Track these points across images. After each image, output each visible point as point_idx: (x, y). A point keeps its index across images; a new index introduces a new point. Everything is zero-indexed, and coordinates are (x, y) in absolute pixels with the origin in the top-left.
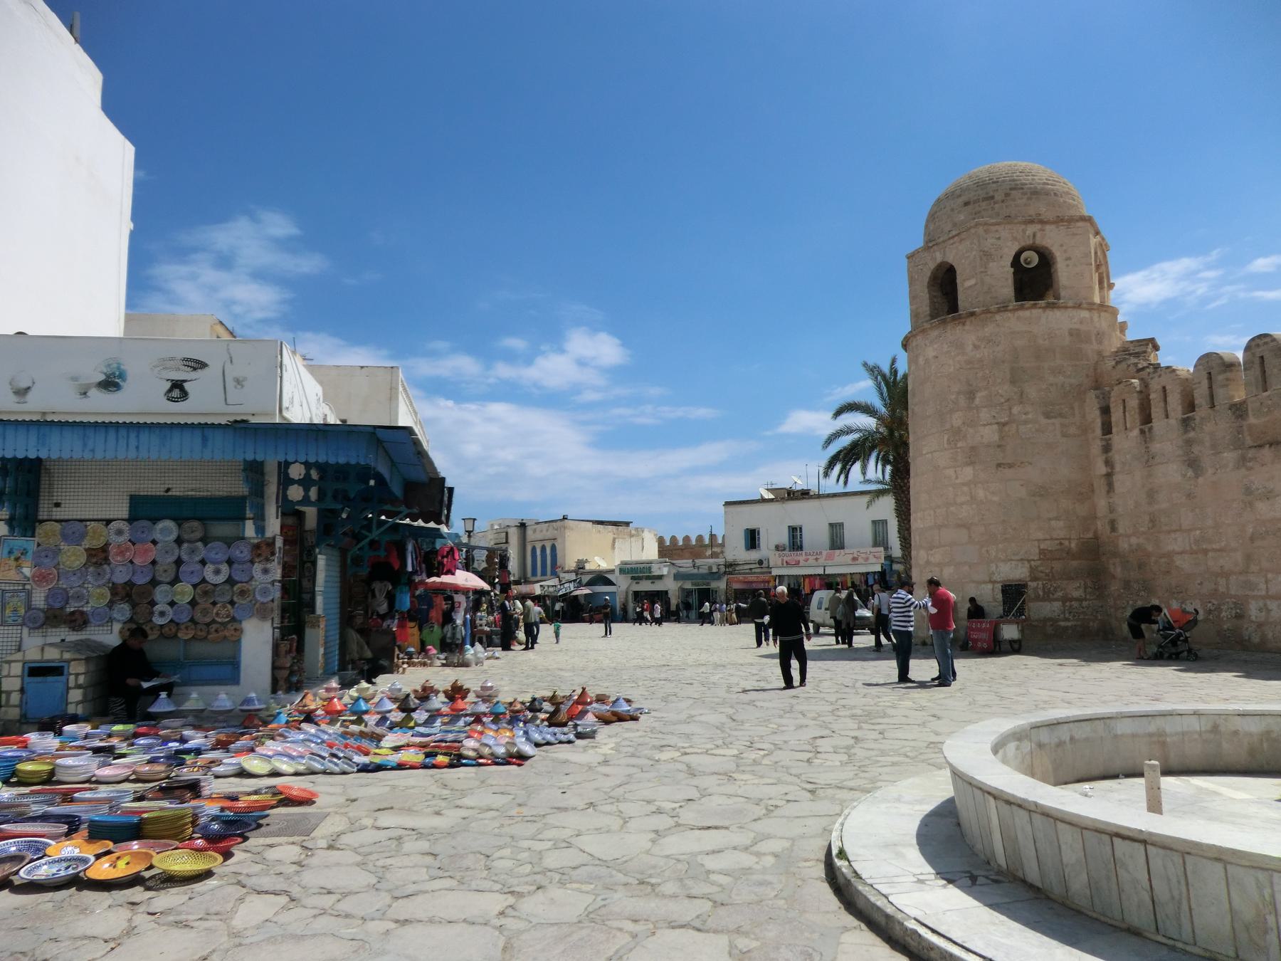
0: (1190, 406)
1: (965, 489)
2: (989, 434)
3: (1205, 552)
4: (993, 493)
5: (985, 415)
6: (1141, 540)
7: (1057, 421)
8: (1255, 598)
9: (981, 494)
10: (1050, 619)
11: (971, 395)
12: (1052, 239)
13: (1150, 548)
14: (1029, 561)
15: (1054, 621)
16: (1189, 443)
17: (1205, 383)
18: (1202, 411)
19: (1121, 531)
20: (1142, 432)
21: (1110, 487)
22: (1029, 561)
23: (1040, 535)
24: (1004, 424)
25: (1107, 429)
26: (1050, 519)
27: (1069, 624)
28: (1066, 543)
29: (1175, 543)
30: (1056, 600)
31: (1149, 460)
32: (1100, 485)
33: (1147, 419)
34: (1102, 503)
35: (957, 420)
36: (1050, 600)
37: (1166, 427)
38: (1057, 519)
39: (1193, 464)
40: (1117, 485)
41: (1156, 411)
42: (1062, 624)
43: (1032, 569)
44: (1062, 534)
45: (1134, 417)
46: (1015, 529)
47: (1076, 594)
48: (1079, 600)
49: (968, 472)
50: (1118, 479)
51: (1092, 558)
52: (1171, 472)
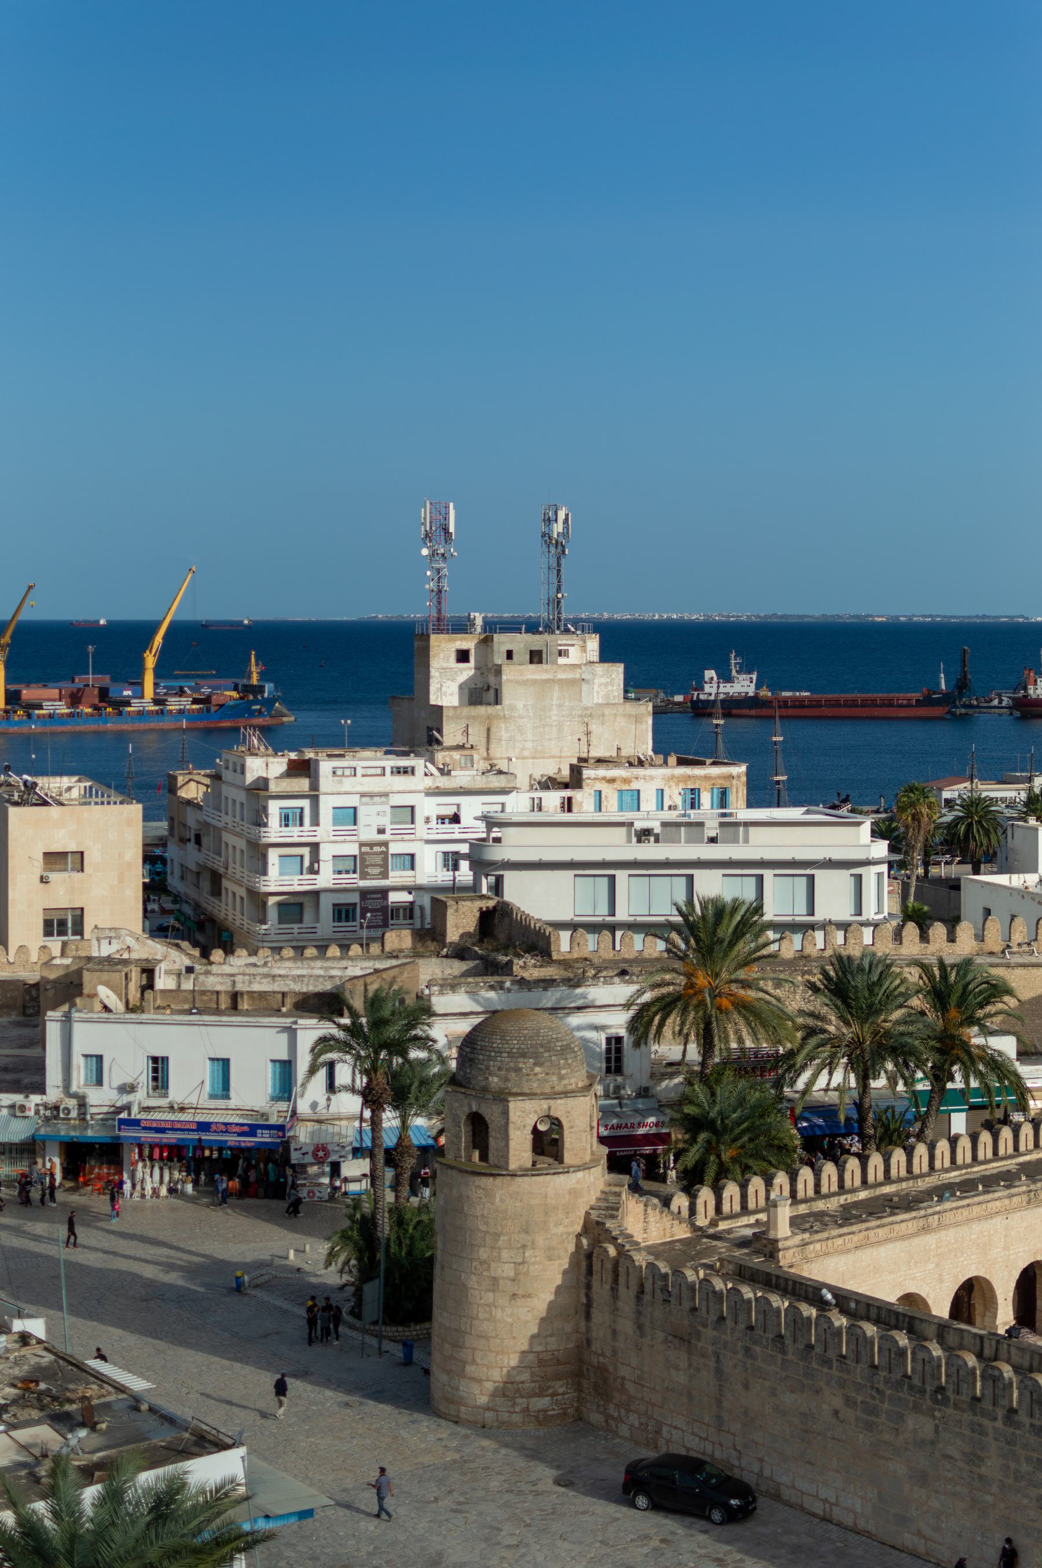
0: (641, 1291)
1: (488, 1309)
3: (643, 1386)
6: (606, 1361)
8: (667, 1425)
10: (542, 1410)
12: (560, 1108)
13: (611, 1369)
14: (531, 1368)
15: (545, 1411)
16: (639, 1313)
17: (651, 1280)
18: (647, 1298)
19: (593, 1348)
20: (612, 1289)
21: (588, 1317)
22: (531, 1368)
24: (519, 1264)
26: (547, 1337)
27: (555, 1413)
28: (556, 1353)
29: (624, 1371)
30: (547, 1396)
31: (614, 1310)
33: (616, 1280)
38: (552, 1335)
39: (640, 1327)
40: (593, 1316)
41: (622, 1280)
42: (550, 1413)
43: (532, 1375)
44: (554, 1347)
45: (608, 1276)
47: (561, 1390)
48: (563, 1394)
50: (595, 1313)
52: (627, 1326)
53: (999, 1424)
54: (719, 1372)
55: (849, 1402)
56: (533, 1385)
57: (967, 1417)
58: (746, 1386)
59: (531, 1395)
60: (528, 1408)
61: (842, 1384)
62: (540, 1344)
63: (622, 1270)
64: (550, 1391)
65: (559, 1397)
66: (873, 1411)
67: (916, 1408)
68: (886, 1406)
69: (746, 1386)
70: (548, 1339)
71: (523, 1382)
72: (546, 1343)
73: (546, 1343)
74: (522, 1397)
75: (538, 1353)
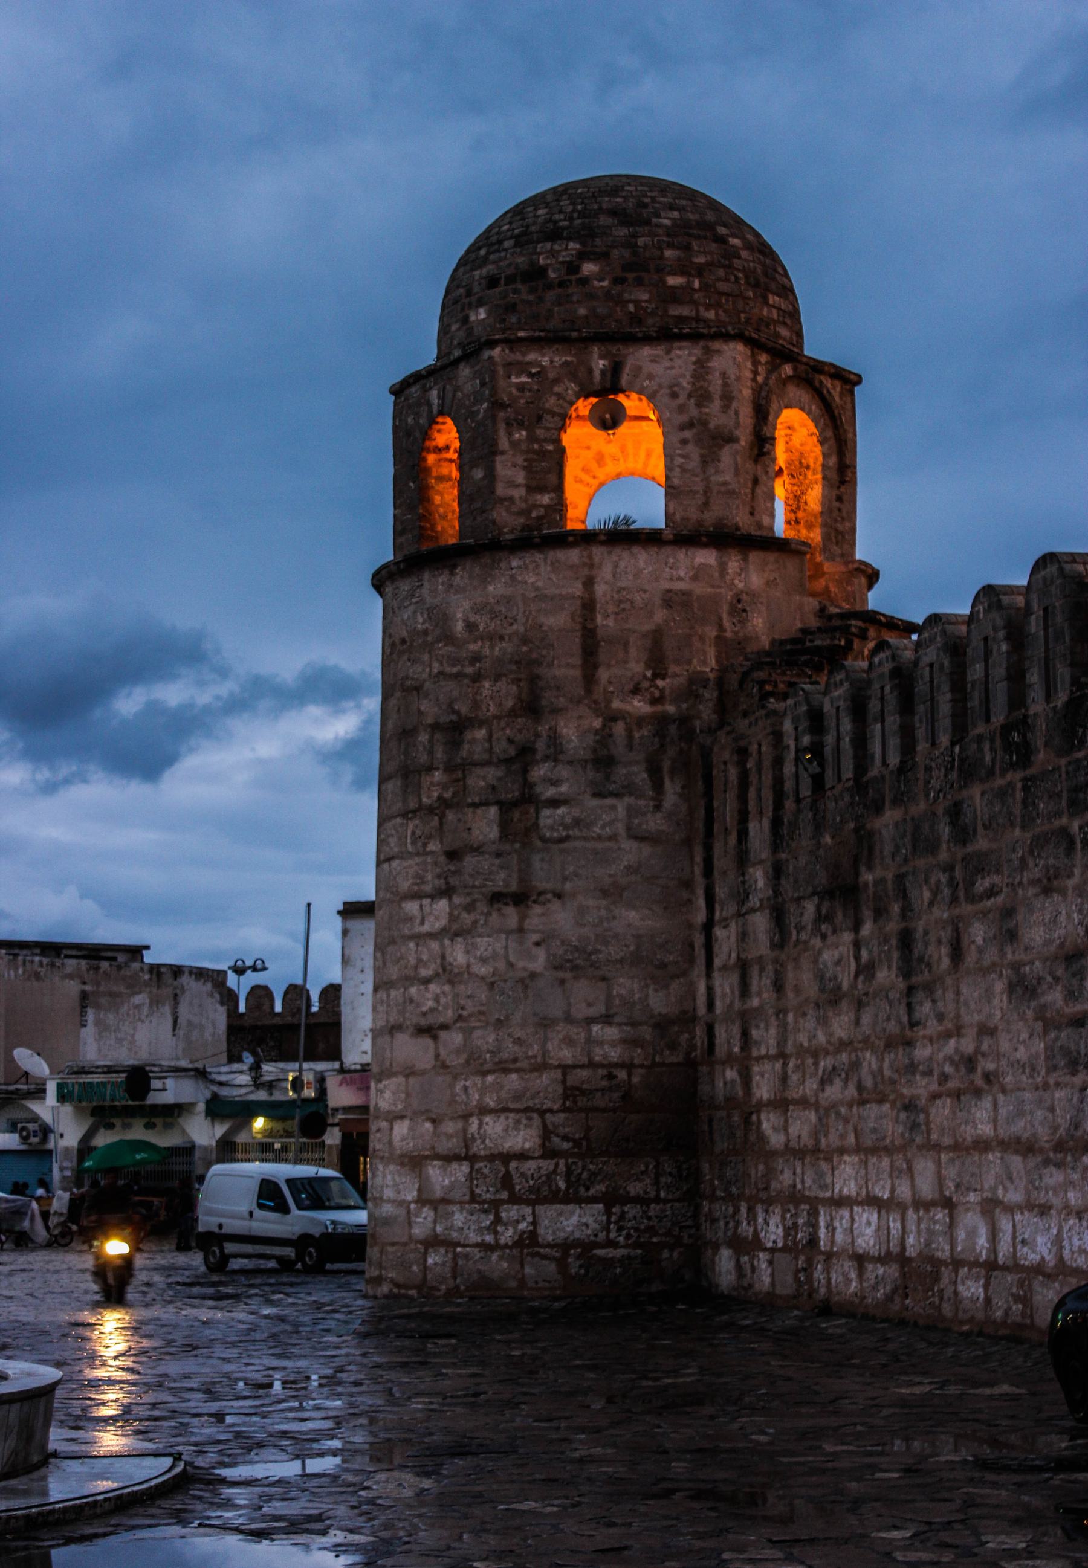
4: (483, 960)
5: (480, 780)
7: (621, 806)
9: (458, 955)
14: (542, 1113)
22: (542, 1113)
23: (567, 1055)
26: (590, 1021)
28: (622, 1075)
30: (593, 1200)
36: (579, 1201)
38: (607, 1019)
42: (600, 1252)
43: (546, 1133)
44: (614, 1054)
46: (518, 1041)
56: (547, 1165)
59: (542, 1195)
60: (533, 1234)
62: (569, 1041)
64: (599, 1188)
65: (631, 1210)
70: (596, 1028)
71: (522, 1156)
72: (589, 1040)
73: (589, 1040)
74: (515, 1199)
75: (565, 1069)
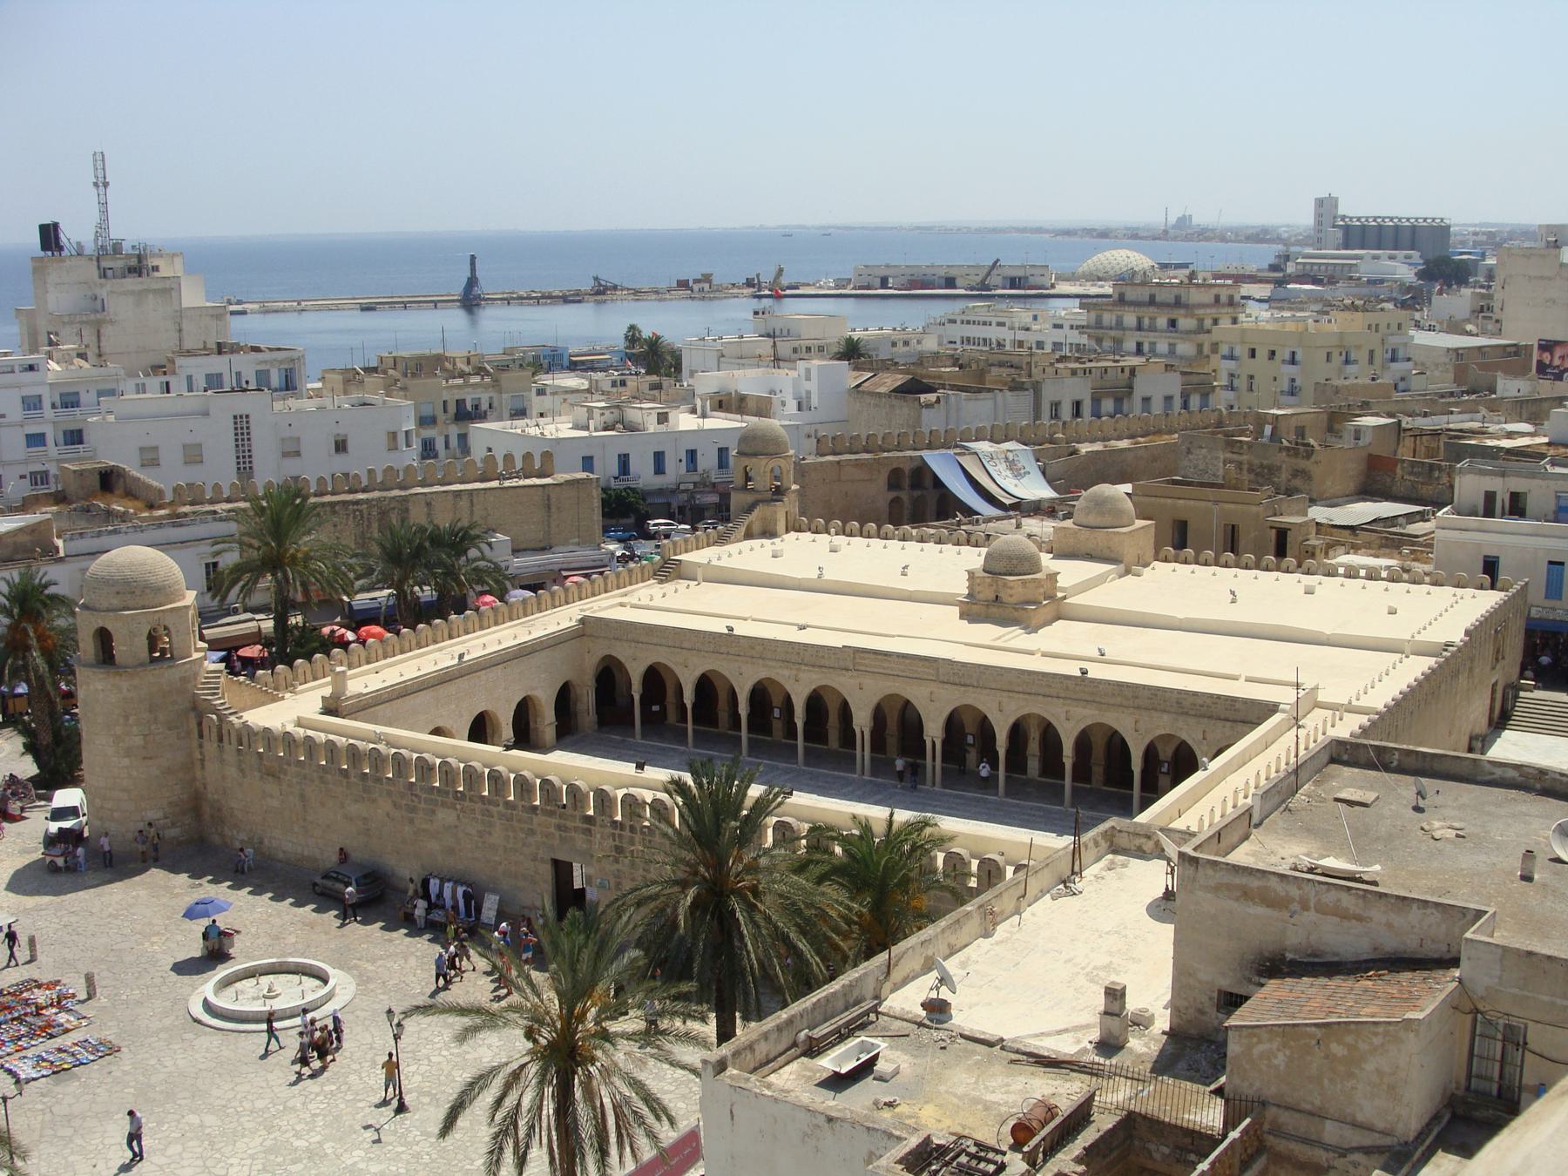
2: (139, 741)
11: (127, 718)
21: (203, 767)
25: (201, 736)
31: (222, 761)
32: (198, 764)
33: (221, 740)
34: (199, 774)
35: (118, 730)
37: (230, 749)
39: (242, 771)
41: (226, 739)
49: (126, 761)
51: (196, 805)
52: (232, 771)
53: (501, 808)
54: (302, 797)
55: (395, 805)
57: (478, 806)
58: (323, 804)
61: (389, 793)
63: (224, 732)
66: (413, 810)
67: (443, 804)
68: (422, 805)
69: (323, 804)
